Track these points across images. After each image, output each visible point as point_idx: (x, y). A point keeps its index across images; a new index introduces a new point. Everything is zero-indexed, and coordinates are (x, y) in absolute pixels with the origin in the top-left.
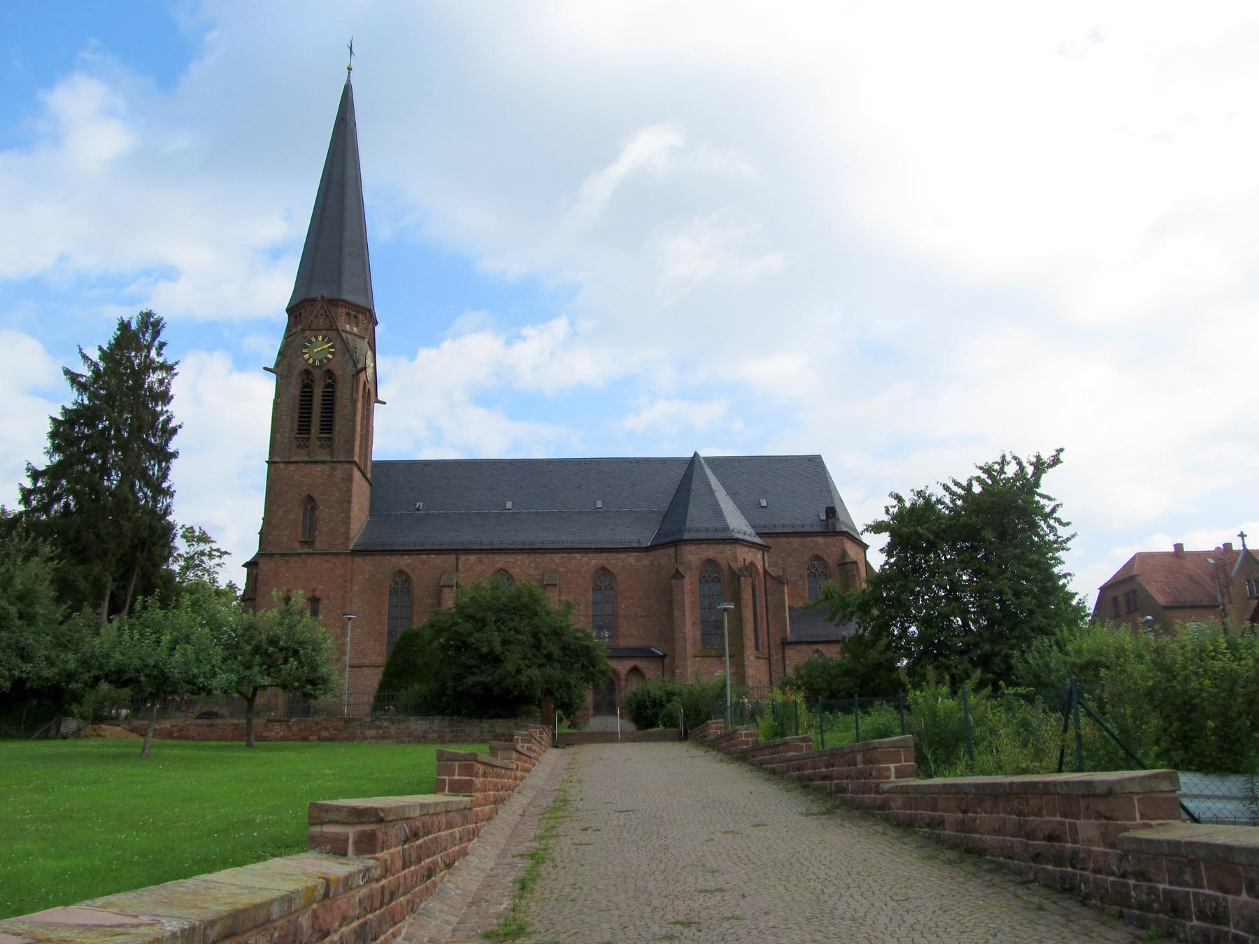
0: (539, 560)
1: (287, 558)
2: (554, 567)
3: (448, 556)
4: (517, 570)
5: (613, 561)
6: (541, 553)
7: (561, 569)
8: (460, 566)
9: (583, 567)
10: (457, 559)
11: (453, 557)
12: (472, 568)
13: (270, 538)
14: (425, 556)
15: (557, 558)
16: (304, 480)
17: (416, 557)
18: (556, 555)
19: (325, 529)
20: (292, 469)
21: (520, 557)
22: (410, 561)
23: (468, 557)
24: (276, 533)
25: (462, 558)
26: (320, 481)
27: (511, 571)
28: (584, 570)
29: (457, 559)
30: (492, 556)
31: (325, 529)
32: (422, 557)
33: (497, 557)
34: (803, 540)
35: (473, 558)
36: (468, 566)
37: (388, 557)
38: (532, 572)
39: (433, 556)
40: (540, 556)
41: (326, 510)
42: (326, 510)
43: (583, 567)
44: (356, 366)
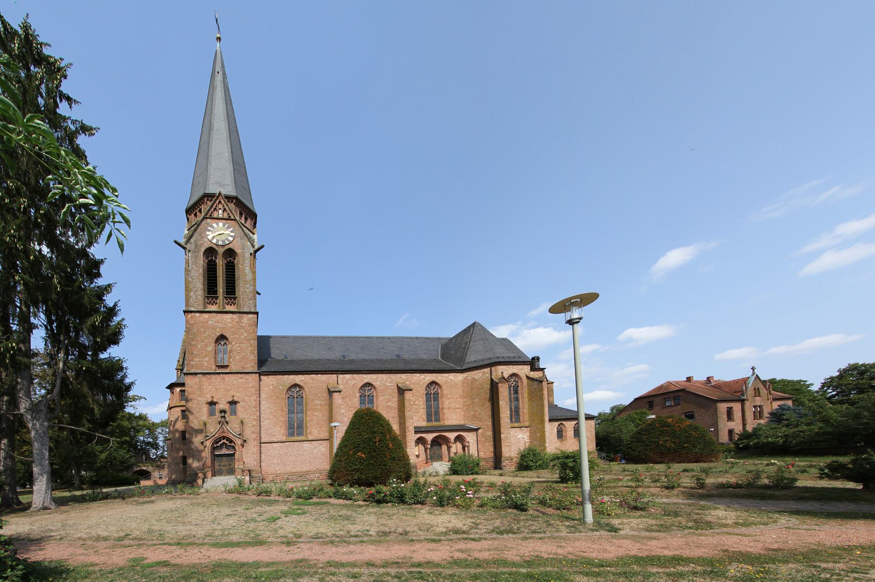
0: (394, 377)
1: (209, 376)
4: (378, 383)
5: (440, 378)
6: (395, 373)
7: (407, 383)
9: (421, 381)
11: (335, 376)
13: (192, 363)
15: (404, 376)
21: (380, 375)
22: (303, 379)
23: (345, 375)
24: (197, 360)
25: (341, 376)
26: (230, 325)
27: (374, 384)
28: (422, 383)
35: (348, 376)
36: (345, 381)
38: (388, 384)
39: (320, 375)
41: (238, 345)
42: (238, 345)
43: (421, 381)
44: (253, 247)
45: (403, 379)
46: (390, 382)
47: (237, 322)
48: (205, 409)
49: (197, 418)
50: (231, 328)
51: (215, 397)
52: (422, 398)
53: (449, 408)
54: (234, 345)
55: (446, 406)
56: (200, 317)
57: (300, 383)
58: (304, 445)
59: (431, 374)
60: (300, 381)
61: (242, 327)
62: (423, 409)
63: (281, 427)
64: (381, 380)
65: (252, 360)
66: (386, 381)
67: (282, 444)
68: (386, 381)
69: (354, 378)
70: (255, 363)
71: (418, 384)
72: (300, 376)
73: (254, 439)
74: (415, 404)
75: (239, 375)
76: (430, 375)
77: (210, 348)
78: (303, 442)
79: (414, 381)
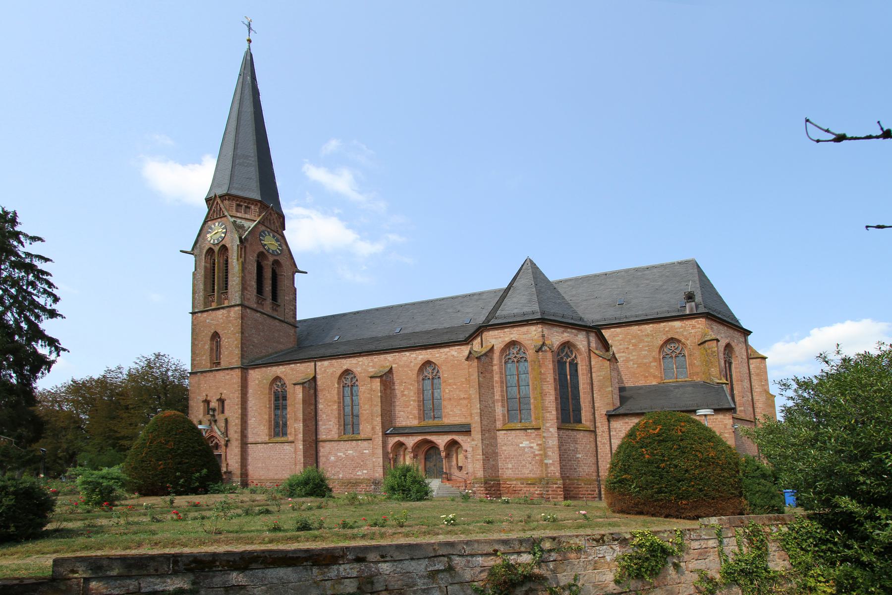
0: (376, 360)
2: (388, 364)
3: (309, 364)
4: (359, 369)
8: (317, 370)
9: (411, 362)
10: (315, 365)
12: (325, 370)
14: (293, 365)
16: (212, 322)
17: (287, 366)
18: (389, 355)
19: (226, 353)
20: (205, 316)
21: (361, 359)
22: (284, 370)
23: (323, 362)
24: (198, 359)
25: (319, 364)
27: (354, 370)
29: (315, 365)
30: (340, 360)
31: (226, 353)
32: (291, 366)
33: (344, 361)
34: (655, 326)
35: (326, 363)
36: (323, 369)
37: (269, 368)
39: (298, 365)
40: (376, 356)
41: (226, 340)
42: (226, 340)
43: (411, 362)
45: (388, 360)
46: (373, 367)
47: (226, 317)
48: (202, 408)
49: (196, 416)
50: (222, 324)
51: (209, 395)
52: (413, 385)
53: (450, 399)
54: (225, 342)
55: (447, 396)
56: (201, 317)
57: (281, 375)
58: (285, 448)
59: (424, 351)
60: (282, 373)
61: (230, 322)
62: (414, 401)
63: (264, 426)
64: (362, 365)
65: (237, 354)
66: (368, 366)
67: (265, 446)
68: (368, 366)
69: (332, 365)
70: (239, 358)
71: (408, 366)
72: (281, 367)
73: (237, 440)
74: (403, 395)
75: (227, 372)
76: (424, 352)
77: (207, 347)
78: (283, 445)
79: (401, 363)
